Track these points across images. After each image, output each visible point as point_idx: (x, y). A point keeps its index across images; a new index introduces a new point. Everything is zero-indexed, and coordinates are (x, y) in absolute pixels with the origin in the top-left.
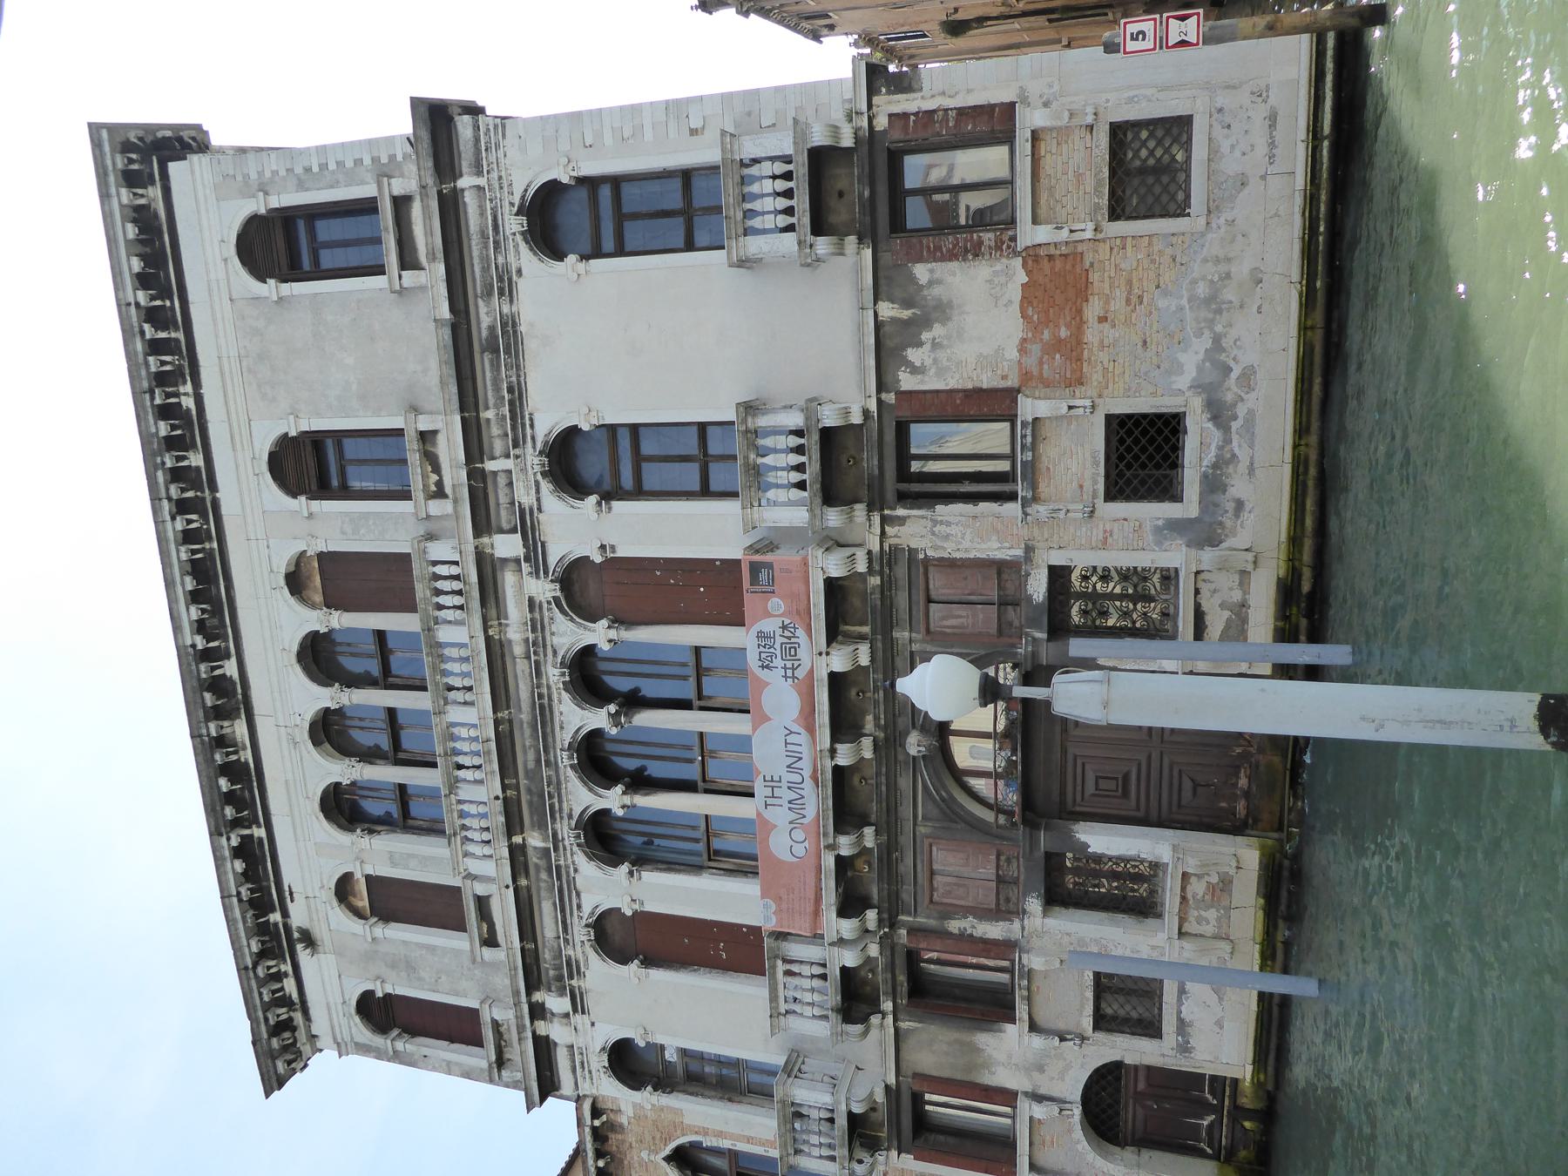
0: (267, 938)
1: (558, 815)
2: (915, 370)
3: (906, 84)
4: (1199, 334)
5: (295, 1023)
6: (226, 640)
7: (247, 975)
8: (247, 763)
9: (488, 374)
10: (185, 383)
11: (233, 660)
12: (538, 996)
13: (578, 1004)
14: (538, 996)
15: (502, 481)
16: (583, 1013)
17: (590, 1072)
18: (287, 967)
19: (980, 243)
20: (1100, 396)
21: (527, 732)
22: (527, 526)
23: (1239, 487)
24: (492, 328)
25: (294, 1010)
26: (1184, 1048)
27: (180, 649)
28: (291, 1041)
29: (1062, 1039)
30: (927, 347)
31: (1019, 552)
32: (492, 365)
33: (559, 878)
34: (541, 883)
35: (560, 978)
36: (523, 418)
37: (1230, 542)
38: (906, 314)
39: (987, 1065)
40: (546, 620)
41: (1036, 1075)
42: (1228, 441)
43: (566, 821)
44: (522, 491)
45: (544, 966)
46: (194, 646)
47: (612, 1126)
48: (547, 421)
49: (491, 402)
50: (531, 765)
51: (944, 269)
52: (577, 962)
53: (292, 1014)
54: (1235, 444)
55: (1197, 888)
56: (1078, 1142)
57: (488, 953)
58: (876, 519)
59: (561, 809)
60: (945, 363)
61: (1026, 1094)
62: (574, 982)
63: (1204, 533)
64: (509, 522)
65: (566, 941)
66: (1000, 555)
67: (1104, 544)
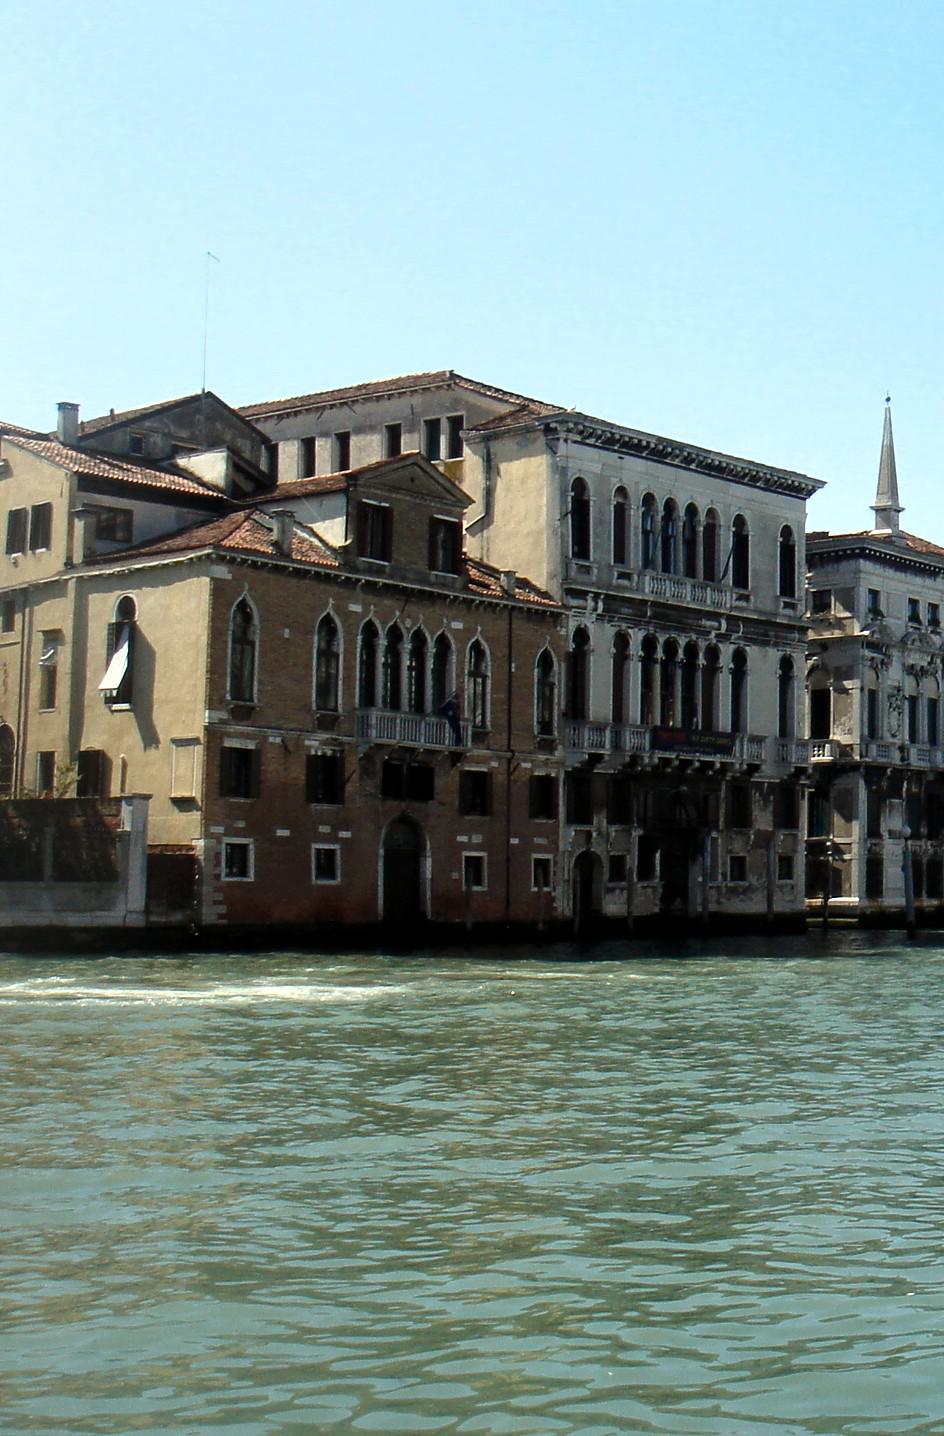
13: (600, 618)
24: (767, 636)
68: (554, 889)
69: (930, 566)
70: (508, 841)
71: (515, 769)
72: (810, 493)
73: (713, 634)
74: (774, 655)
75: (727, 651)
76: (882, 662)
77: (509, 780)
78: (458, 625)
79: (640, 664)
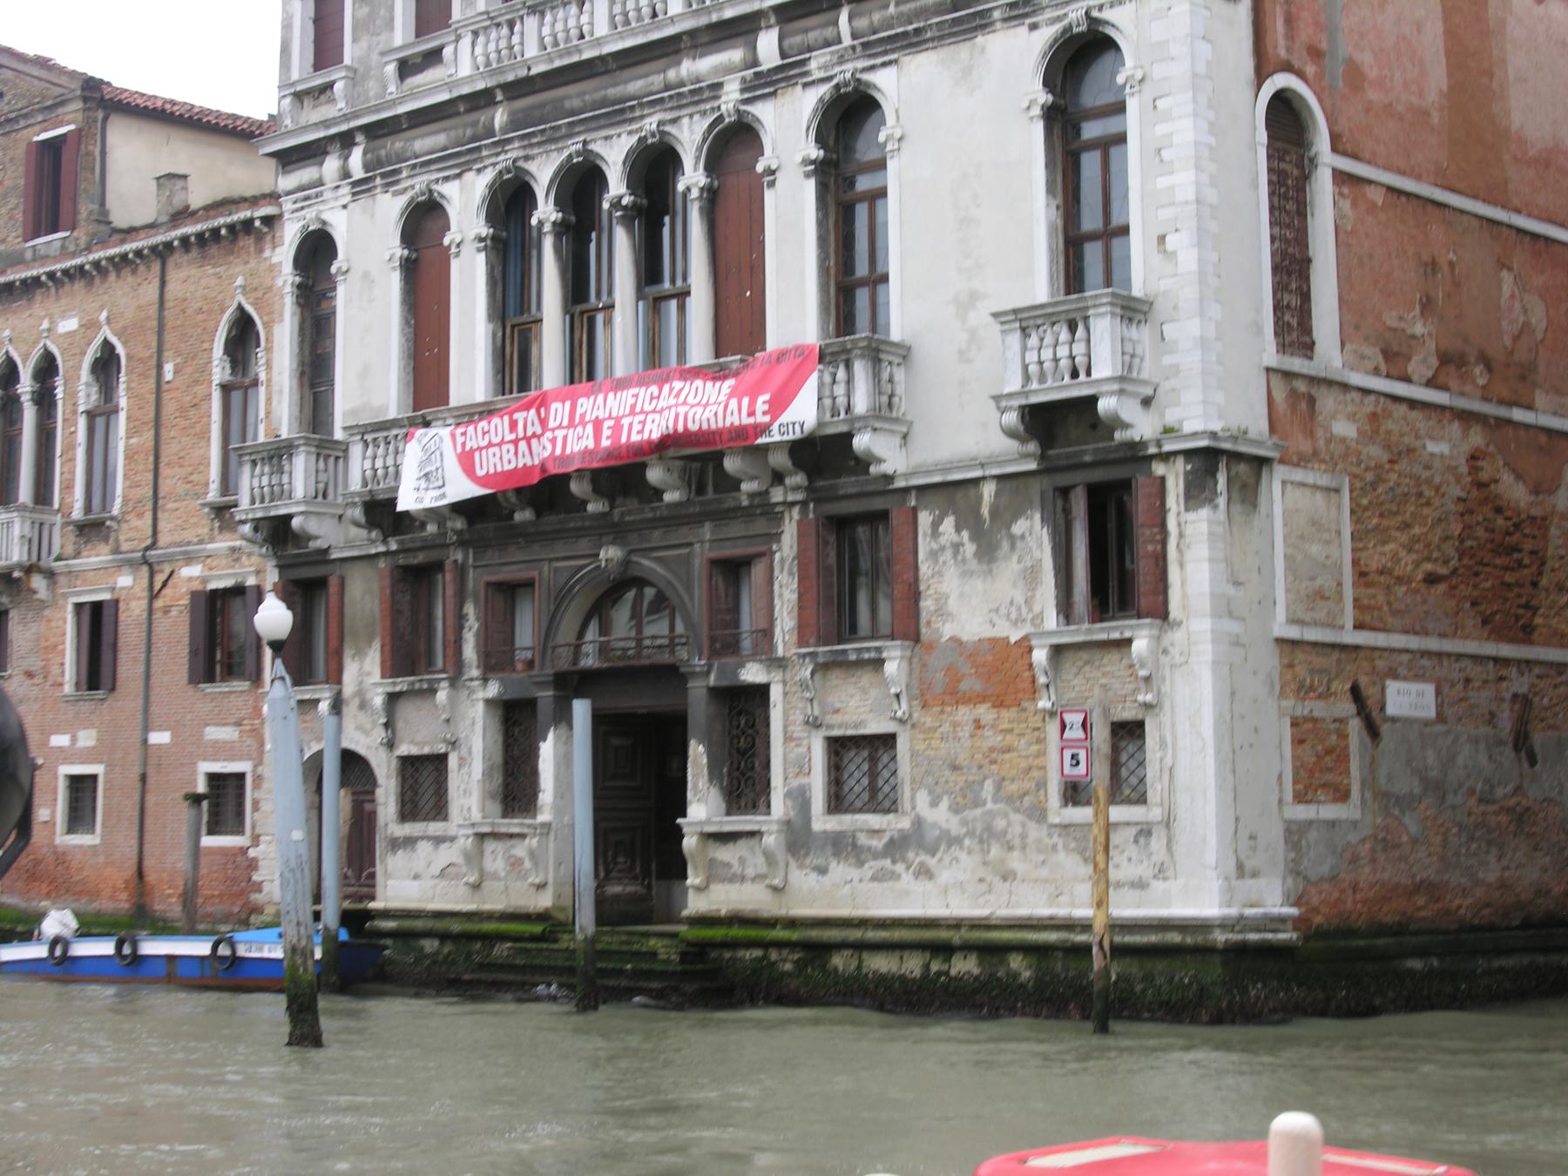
1: (526, 143)
2: (936, 525)
3: (1193, 492)
4: (964, 823)
12: (360, 138)
13: (361, 188)
14: (360, 138)
15: (829, 32)
16: (354, 194)
17: (302, 208)
20: (913, 726)
21: (598, 95)
22: (787, 74)
23: (840, 871)
26: (395, 844)
29: (386, 725)
30: (955, 538)
31: (780, 652)
33: (470, 151)
34: (461, 127)
36: (893, 51)
37: (793, 864)
38: (985, 511)
40: (703, 107)
41: (356, 702)
42: (877, 855)
43: (521, 153)
44: (822, 60)
45: (388, 142)
47: (260, 238)
48: (886, 82)
50: (568, 104)
52: (397, 182)
54: (872, 863)
57: (391, 69)
58: (799, 496)
59: (532, 146)
60: (941, 560)
61: (339, 693)
62: (378, 181)
63: (799, 839)
64: (791, 47)
65: (414, 167)
67: (788, 738)
68: (256, 840)
70: (145, 741)
77: (151, 611)
78: (69, 325)
79: (482, 257)
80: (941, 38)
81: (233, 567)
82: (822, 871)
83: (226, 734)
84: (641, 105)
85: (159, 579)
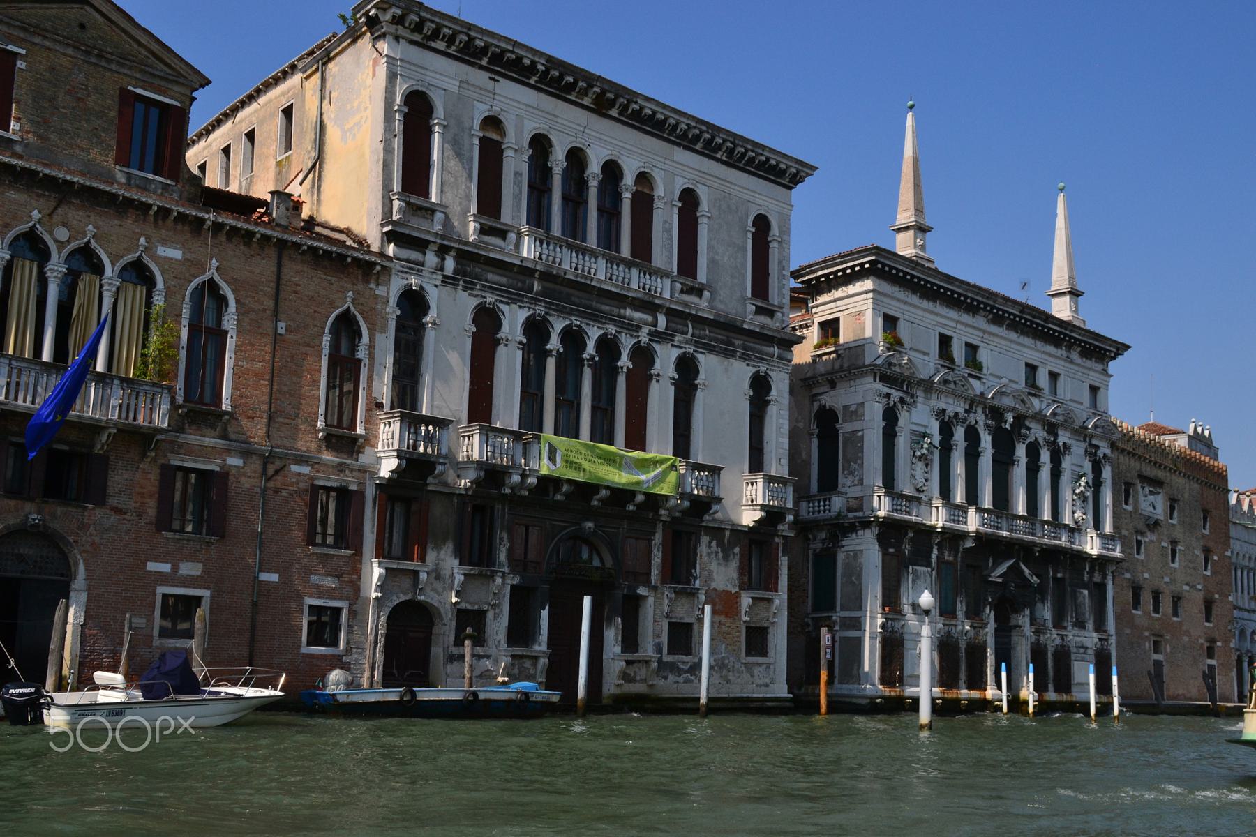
0: (478, 50)
2: (710, 542)
5: (416, 34)
6: (627, 118)
7: (465, 28)
8: (570, 94)
9: (720, 337)
10: (726, 157)
11: (617, 116)
13: (448, 281)
16: (442, 281)
18: (452, 51)
19: (745, 575)
21: (588, 303)
23: (672, 678)
24: (733, 345)
25: (423, 39)
27: (637, 94)
28: (407, 25)
32: (723, 340)
35: (464, 274)
36: (704, 349)
38: (726, 542)
39: (438, 547)
40: (631, 332)
41: (434, 574)
46: (636, 103)
49: (712, 335)
50: (573, 299)
51: (737, 557)
53: (423, 36)
55: (528, 664)
56: (398, 598)
62: (461, 283)
65: (484, 286)
66: (652, 574)
69: (966, 297)
71: (277, 472)
72: (796, 180)
73: (645, 330)
74: (742, 372)
75: (666, 359)
76: (902, 400)
80: (720, 353)
81: (338, 475)
82: (666, 678)
83: (330, 583)
84: (606, 318)
85: (271, 469)
